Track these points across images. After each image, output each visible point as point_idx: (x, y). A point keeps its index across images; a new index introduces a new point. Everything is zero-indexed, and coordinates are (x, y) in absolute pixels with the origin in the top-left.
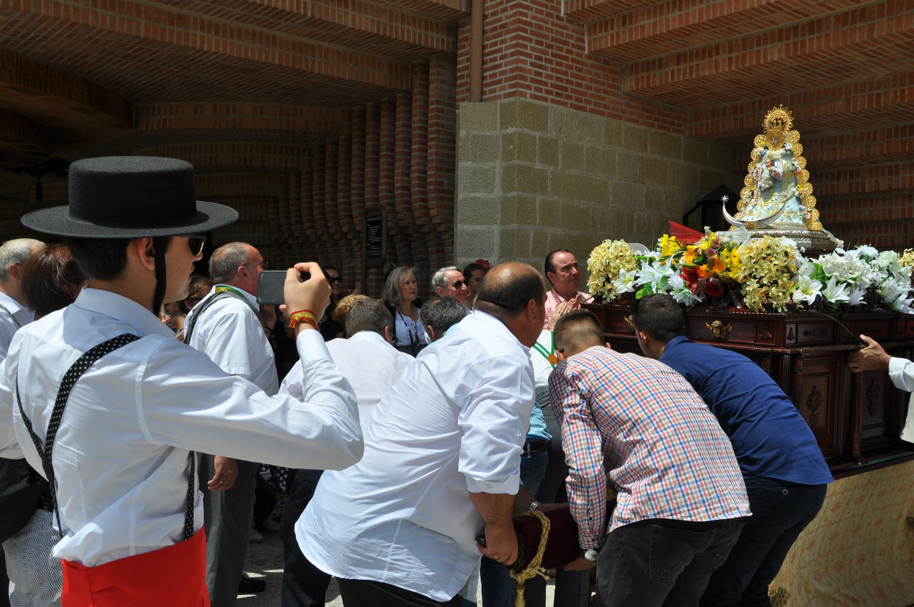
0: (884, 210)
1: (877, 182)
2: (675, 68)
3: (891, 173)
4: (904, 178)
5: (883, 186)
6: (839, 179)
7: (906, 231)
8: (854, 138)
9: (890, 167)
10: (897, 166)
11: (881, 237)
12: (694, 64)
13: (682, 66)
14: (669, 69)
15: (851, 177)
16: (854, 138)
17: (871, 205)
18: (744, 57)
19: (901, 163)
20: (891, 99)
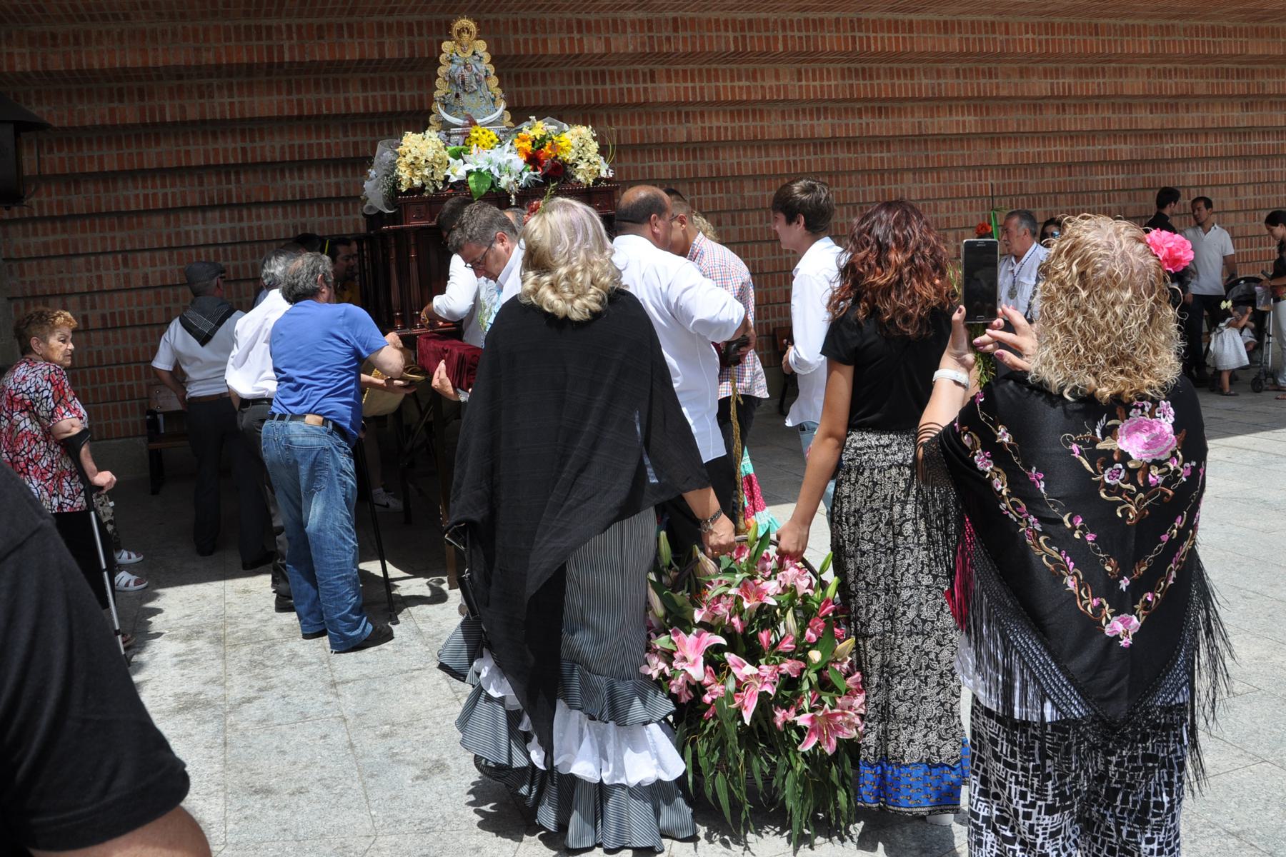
0: (178, 152)
1: (182, 108)
3: (202, 96)
4: (222, 105)
5: (193, 114)
6: (121, 101)
7: (201, 184)
8: (174, 34)
11: (165, 195)
15: (142, 98)
16: (174, 34)
17: (158, 143)
19: (215, 81)
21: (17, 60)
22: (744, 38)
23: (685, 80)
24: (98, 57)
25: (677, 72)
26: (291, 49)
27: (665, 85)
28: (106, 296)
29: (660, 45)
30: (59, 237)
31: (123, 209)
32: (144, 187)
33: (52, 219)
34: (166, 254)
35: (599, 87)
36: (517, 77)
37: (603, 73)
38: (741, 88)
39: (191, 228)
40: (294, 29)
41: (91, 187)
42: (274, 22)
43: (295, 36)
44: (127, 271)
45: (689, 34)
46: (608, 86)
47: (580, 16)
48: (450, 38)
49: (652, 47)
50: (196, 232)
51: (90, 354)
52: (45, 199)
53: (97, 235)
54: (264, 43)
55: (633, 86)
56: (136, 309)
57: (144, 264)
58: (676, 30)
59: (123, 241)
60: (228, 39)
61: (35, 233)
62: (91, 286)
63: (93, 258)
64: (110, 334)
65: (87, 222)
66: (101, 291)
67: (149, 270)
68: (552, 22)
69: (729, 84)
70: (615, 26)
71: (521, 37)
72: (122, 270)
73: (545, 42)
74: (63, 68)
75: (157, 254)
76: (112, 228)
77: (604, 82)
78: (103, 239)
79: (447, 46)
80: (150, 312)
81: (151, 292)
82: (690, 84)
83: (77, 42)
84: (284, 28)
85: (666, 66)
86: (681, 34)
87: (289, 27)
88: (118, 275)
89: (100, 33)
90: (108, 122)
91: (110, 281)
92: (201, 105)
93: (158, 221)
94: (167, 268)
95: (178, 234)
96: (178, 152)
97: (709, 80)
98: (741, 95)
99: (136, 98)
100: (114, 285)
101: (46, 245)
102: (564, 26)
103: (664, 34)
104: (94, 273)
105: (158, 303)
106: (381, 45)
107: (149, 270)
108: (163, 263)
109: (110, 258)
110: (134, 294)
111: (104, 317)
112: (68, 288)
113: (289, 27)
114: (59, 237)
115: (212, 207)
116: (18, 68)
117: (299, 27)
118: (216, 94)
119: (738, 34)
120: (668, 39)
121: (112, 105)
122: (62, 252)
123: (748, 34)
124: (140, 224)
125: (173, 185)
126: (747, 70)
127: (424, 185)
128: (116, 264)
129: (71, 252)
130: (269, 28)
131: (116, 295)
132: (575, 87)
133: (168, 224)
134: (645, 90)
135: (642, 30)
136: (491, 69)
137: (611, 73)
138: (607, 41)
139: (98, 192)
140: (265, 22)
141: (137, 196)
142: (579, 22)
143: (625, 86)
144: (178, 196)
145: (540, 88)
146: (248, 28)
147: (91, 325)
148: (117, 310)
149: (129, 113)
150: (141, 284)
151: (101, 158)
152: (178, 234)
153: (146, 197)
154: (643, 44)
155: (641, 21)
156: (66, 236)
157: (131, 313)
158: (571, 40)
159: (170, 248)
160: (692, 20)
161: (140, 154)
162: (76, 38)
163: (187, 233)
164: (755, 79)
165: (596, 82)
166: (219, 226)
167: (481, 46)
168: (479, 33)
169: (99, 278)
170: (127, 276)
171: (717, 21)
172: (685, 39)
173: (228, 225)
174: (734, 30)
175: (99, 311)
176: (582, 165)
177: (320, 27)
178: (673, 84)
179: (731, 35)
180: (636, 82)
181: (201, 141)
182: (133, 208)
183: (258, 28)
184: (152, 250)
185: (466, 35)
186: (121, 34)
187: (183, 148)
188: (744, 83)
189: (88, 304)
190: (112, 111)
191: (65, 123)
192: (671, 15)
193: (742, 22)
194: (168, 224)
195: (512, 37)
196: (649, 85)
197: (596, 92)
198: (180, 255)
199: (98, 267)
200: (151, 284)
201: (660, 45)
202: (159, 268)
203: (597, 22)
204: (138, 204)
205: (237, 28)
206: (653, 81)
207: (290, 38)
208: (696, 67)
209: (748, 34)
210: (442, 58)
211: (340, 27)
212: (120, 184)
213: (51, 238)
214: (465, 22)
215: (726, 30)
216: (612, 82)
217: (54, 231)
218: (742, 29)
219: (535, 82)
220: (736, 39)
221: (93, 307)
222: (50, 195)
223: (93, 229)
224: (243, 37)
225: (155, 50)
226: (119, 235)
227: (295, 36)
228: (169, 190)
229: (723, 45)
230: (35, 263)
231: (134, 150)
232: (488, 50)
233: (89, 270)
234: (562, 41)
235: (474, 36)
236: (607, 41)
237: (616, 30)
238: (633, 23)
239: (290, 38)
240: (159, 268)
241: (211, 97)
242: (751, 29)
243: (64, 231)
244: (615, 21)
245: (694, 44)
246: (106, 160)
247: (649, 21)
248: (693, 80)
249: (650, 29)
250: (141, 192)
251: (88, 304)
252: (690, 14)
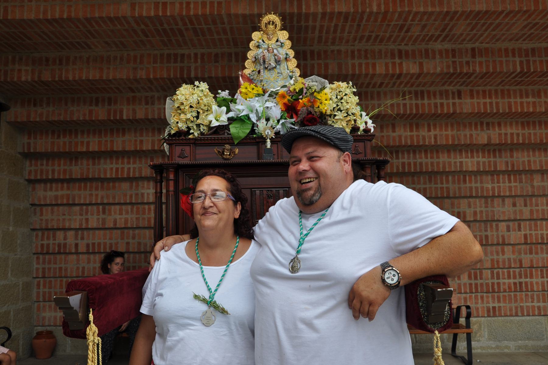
0: (136, 141)
1: (134, 111)
3: (147, 103)
5: (140, 114)
8: (122, 59)
9: (146, 97)
10: (152, 97)
15: (110, 104)
16: (122, 59)
17: (124, 135)
20: (177, 11)
21: (23, 73)
22: (528, 62)
23: (484, 97)
24: (73, 73)
25: (478, 92)
26: (196, 69)
27: (469, 101)
28: (91, 232)
29: (462, 67)
30: (65, 192)
31: (102, 176)
32: (117, 163)
33: (62, 181)
34: (129, 207)
35: (420, 102)
37: (422, 92)
38: (528, 103)
39: (145, 191)
40: (199, 56)
41: (85, 162)
43: (199, 60)
44: (104, 216)
45: (483, 59)
46: (426, 101)
47: (400, 47)
48: (258, 29)
49: (455, 68)
50: (148, 194)
51: (78, 268)
52: (56, 168)
53: (88, 192)
54: (179, 65)
55: (445, 101)
56: (108, 242)
57: (115, 213)
58: (474, 56)
59: (102, 198)
60: (155, 62)
61: (51, 189)
62: (81, 224)
63: (84, 207)
64: (92, 256)
65: (83, 184)
66: (87, 229)
67: (118, 217)
68: (380, 51)
69: (519, 100)
70: (427, 54)
71: (356, 62)
72: (102, 216)
73: (374, 65)
74: (50, 80)
75: (124, 207)
76: (97, 189)
77: (423, 98)
78: (91, 195)
79: (256, 36)
80: (117, 244)
81: (119, 232)
82: (488, 100)
83: (61, 64)
84: (192, 55)
85: (469, 87)
86: (478, 59)
87: (196, 55)
88: (98, 219)
89: (76, 58)
90: (87, 118)
91: (93, 223)
92: (146, 109)
93: (125, 185)
94: (129, 216)
95: (137, 194)
96: (136, 141)
97: (503, 97)
98: (528, 108)
99: (106, 104)
100: (95, 225)
101: (56, 197)
102: (389, 55)
103: (465, 60)
104: (84, 217)
105: (122, 239)
107: (118, 217)
108: (127, 213)
109: (95, 208)
110: (108, 232)
111: (88, 245)
112: (67, 225)
113: (196, 55)
114: (65, 192)
116: (23, 79)
117: (203, 55)
118: (156, 102)
119: (524, 59)
120: (468, 63)
121: (91, 108)
122: (65, 201)
123: (531, 59)
124: (114, 187)
125: (134, 163)
126: (533, 90)
127: (189, 128)
128: (98, 212)
129: (71, 202)
130: (183, 55)
131: (97, 232)
133: (131, 188)
134: (454, 104)
135: (447, 57)
136: (291, 53)
137: (429, 92)
138: (421, 64)
139: (88, 165)
141: (112, 169)
142: (400, 52)
143: (438, 101)
144: (137, 170)
146: (169, 55)
147: (80, 250)
148: (96, 241)
149: (101, 113)
150: (112, 225)
151: (88, 143)
152: (137, 194)
153: (117, 169)
154: (448, 67)
155: (447, 51)
156: (69, 192)
157: (105, 244)
158: (394, 64)
159: (131, 204)
160: (487, 49)
161: (112, 142)
162: (61, 61)
163: (143, 194)
164: (540, 97)
165: (417, 98)
167: (284, 36)
168: (282, 25)
169: (87, 220)
170: (104, 220)
171: (506, 50)
172: (481, 63)
174: (520, 56)
175: (85, 241)
176: (340, 115)
177: (216, 55)
178: (475, 100)
179: (517, 59)
180: (447, 98)
181: (150, 134)
182: (108, 176)
183: (176, 55)
185: (271, 27)
186: (88, 59)
187: (139, 138)
188: (531, 99)
189: (79, 236)
190: (91, 112)
191: (62, 118)
192: (470, 46)
193: (526, 51)
194: (131, 188)
195: (350, 62)
196: (457, 101)
197: (417, 105)
198: (138, 209)
199: (87, 213)
200: (118, 226)
201: (462, 67)
202: (124, 216)
203: (413, 51)
204: (111, 174)
205: (162, 55)
206: (460, 97)
207: (196, 61)
208: (493, 88)
209: (531, 59)
210: (252, 45)
211: (230, 55)
212: (102, 161)
213: (60, 193)
214: (272, 17)
215: (514, 56)
216: (429, 98)
217: (62, 189)
218: (527, 55)
219: (372, 98)
220: (521, 63)
221: (82, 238)
222: (59, 165)
223: (85, 189)
224: (165, 61)
225: (109, 68)
226: (100, 193)
227: (199, 60)
228: (132, 166)
229: (511, 67)
230: (50, 208)
231: (109, 139)
232: (289, 39)
233: (81, 215)
234: (387, 65)
235: (279, 27)
236: (421, 64)
237: (427, 56)
238: (440, 52)
239: (196, 61)
240: (124, 216)
241: (153, 104)
242: (533, 55)
243: (68, 189)
244: (427, 51)
245: (487, 67)
246: (91, 144)
247: (453, 50)
248: (490, 97)
249: (454, 56)
250: (114, 166)
251: (79, 236)
252: (485, 45)
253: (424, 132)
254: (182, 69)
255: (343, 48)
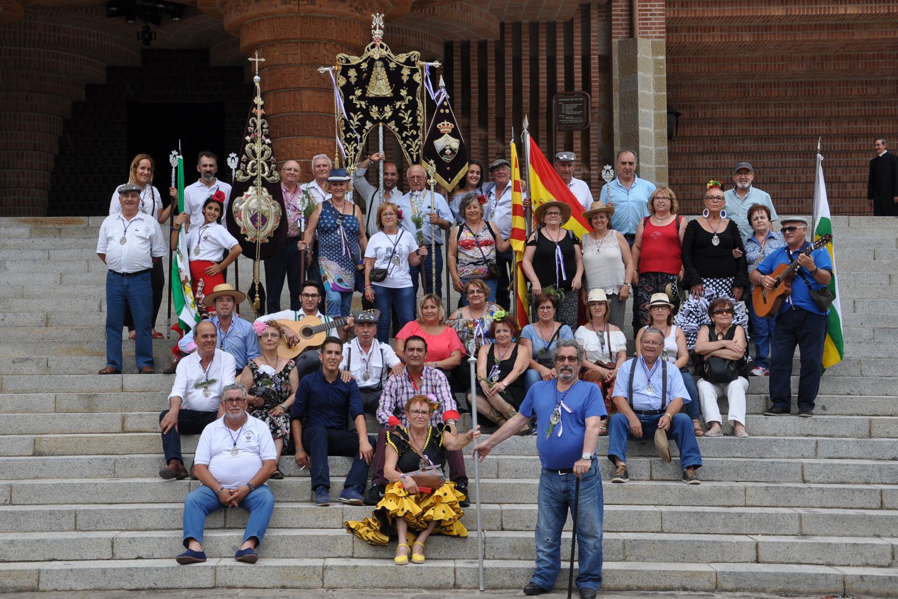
1: (705, 113)
2: (687, 34)
12: (699, 33)
13: (691, 34)
14: (683, 34)
18: (730, 36)
19: (718, 103)
36: (838, 104)
39: (697, 161)
42: (747, 81)
46: (878, 108)
71: (841, 87)
73: (851, 90)
106: (786, 91)
115: (707, 153)
130: (745, 84)
132: (863, 108)
138: (878, 89)
140: (744, 81)
142: (866, 82)
143: (886, 107)
145: (848, 108)
166: (708, 161)
173: (712, 161)
184: (681, 169)
211: (771, 84)
236: (878, 89)
250: (681, 145)
253: (875, 126)
254: (744, 92)
255: (834, 80)
